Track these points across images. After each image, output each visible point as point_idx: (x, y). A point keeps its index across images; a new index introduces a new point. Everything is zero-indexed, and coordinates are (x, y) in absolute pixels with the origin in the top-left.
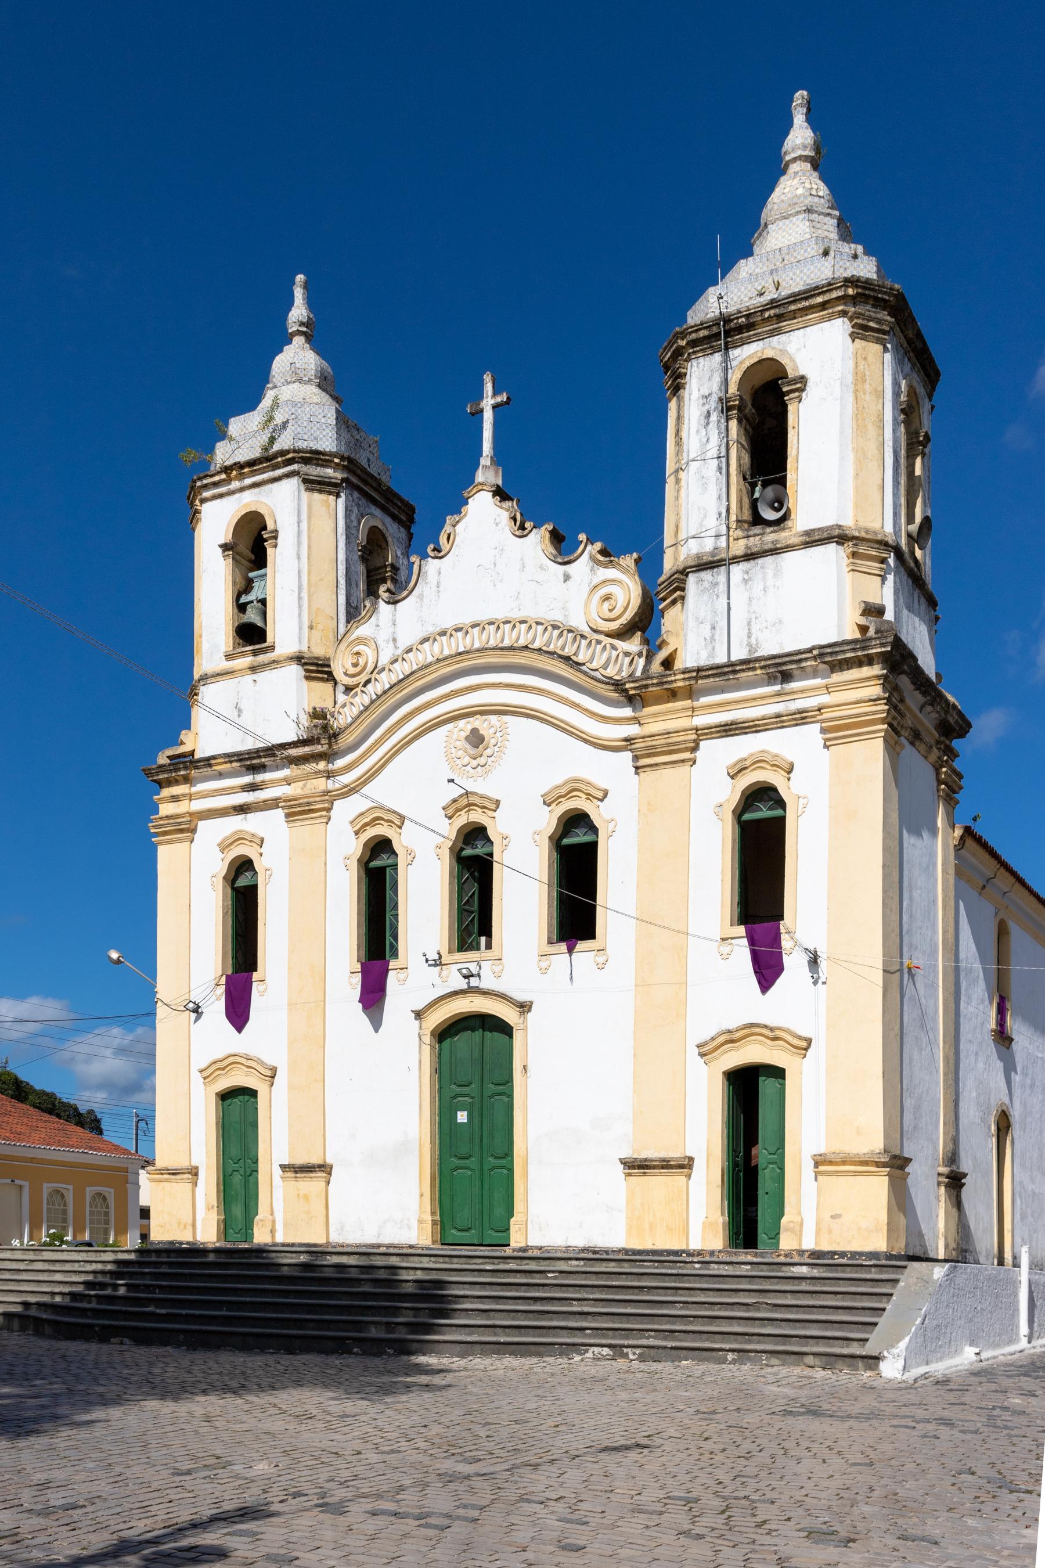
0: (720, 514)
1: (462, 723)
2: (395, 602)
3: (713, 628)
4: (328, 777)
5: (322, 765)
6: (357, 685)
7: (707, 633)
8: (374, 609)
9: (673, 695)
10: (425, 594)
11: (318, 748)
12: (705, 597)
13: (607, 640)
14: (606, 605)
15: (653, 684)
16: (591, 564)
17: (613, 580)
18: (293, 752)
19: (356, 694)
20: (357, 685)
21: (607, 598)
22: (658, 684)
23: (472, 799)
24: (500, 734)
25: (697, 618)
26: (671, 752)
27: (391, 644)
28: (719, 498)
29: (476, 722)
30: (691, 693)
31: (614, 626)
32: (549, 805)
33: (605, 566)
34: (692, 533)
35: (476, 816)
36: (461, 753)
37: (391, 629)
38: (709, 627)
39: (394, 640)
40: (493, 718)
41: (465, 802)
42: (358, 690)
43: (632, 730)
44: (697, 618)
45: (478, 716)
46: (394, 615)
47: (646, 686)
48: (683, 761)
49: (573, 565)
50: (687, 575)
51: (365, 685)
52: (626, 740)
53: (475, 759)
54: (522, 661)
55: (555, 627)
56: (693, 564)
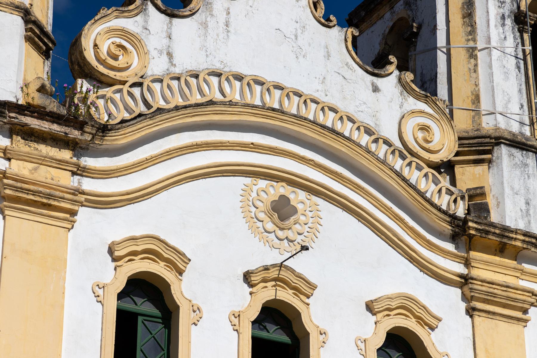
0: (522, 106)
1: (263, 183)
2: (172, 16)
3: (528, 203)
4: (74, 173)
5: (66, 155)
6: (124, 83)
7: (524, 207)
8: (142, 10)
9: (501, 250)
10: (210, 24)
11: (75, 134)
12: (518, 172)
13: (426, 169)
14: (420, 135)
15: (494, 233)
16: (401, 88)
17: (431, 115)
18: (34, 123)
19: (120, 91)
20: (124, 83)
21: (424, 128)
22: (498, 235)
23: (284, 274)
24: (310, 214)
25: (512, 189)
26: (505, 306)
27: (165, 58)
28: (520, 91)
29: (283, 189)
30: (517, 255)
31: (435, 158)
32: (374, 314)
33: (417, 97)
34: (499, 109)
35: (286, 295)
36: (262, 216)
37: (166, 41)
38: (523, 201)
39: (170, 55)
40: (302, 195)
41: (273, 273)
42: (126, 88)
43: (460, 269)
44: (512, 189)
45: (284, 184)
46: (170, 28)
47: (487, 232)
48: (519, 320)
49: (380, 80)
50: (498, 144)
51: (131, 86)
52: (461, 276)
53: (282, 229)
54: (343, 149)
55: (369, 132)
56: (509, 137)
